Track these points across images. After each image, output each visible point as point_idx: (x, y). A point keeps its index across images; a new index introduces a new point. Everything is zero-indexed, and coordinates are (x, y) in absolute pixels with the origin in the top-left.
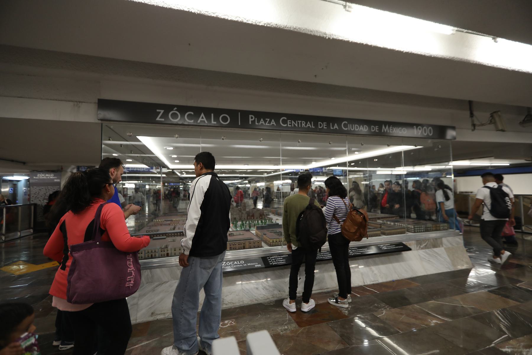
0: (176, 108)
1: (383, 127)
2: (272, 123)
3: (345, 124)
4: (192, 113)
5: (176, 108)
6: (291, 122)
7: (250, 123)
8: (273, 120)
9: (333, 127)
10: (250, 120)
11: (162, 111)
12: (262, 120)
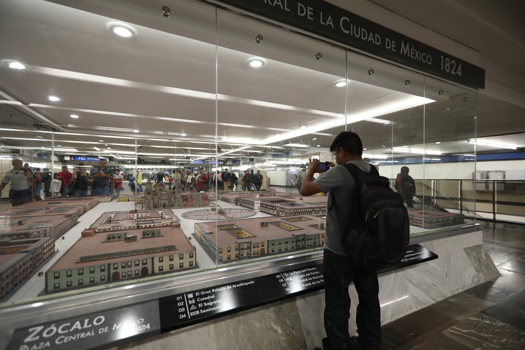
1: (403, 45)
3: (345, 21)
9: (325, 20)
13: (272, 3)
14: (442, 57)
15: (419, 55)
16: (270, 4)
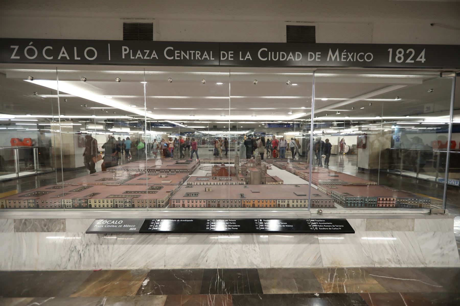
0: (31, 43)
1: (330, 53)
2: (152, 56)
4: (51, 48)
5: (31, 43)
6: (180, 53)
7: (123, 57)
8: (154, 52)
9: (243, 57)
10: (124, 53)
11: (17, 47)
12: (139, 52)
13: (201, 58)
14: (391, 50)
15: (353, 57)
16: (200, 59)
